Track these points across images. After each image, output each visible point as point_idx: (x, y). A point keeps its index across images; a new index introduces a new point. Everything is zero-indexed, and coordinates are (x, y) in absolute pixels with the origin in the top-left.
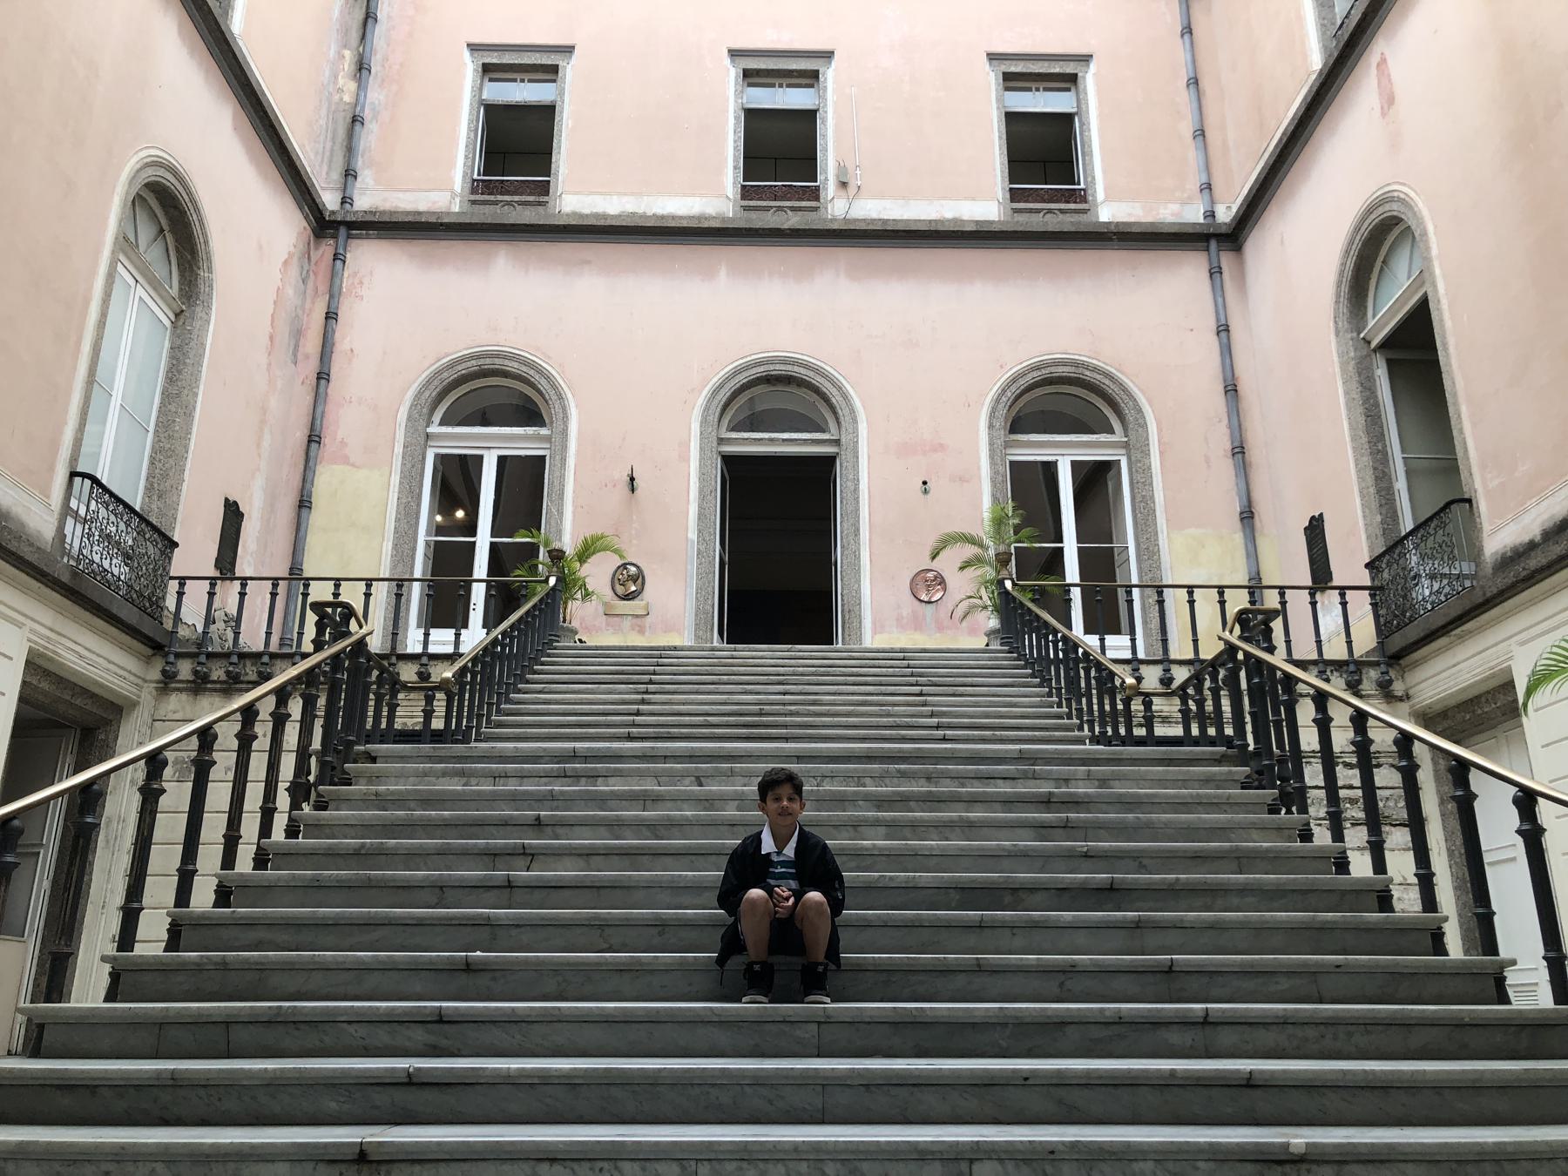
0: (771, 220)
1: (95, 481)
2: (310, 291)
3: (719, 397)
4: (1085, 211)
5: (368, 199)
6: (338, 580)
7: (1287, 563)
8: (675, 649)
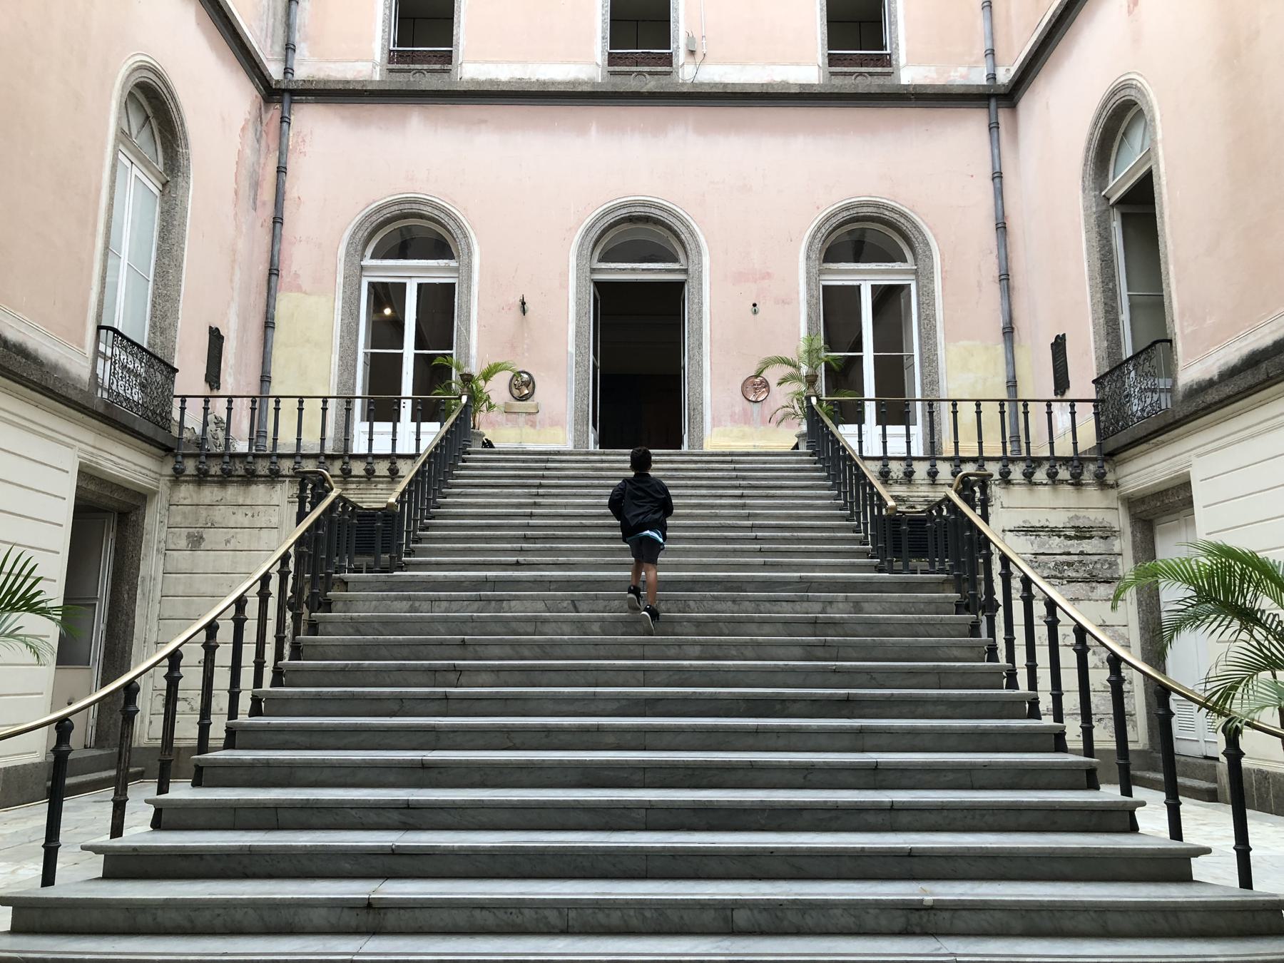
0: (632, 84)
1: (115, 331)
4: (889, 74)
5: (306, 69)
8: (558, 453)
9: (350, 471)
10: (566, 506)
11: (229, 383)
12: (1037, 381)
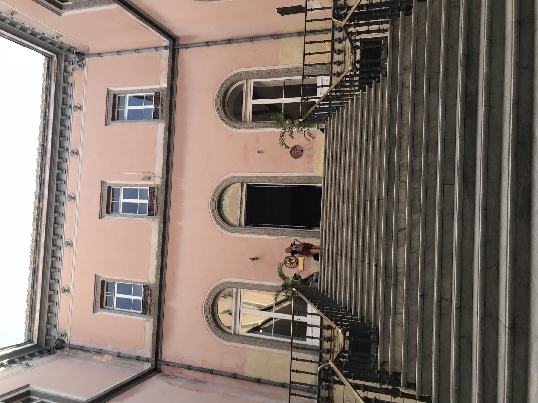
0: (161, 205)
2: (180, 375)
3: (225, 226)
4: (163, 93)
5: (147, 352)
6: (291, 370)
7: (296, 22)
9: (328, 349)
10: (347, 240)
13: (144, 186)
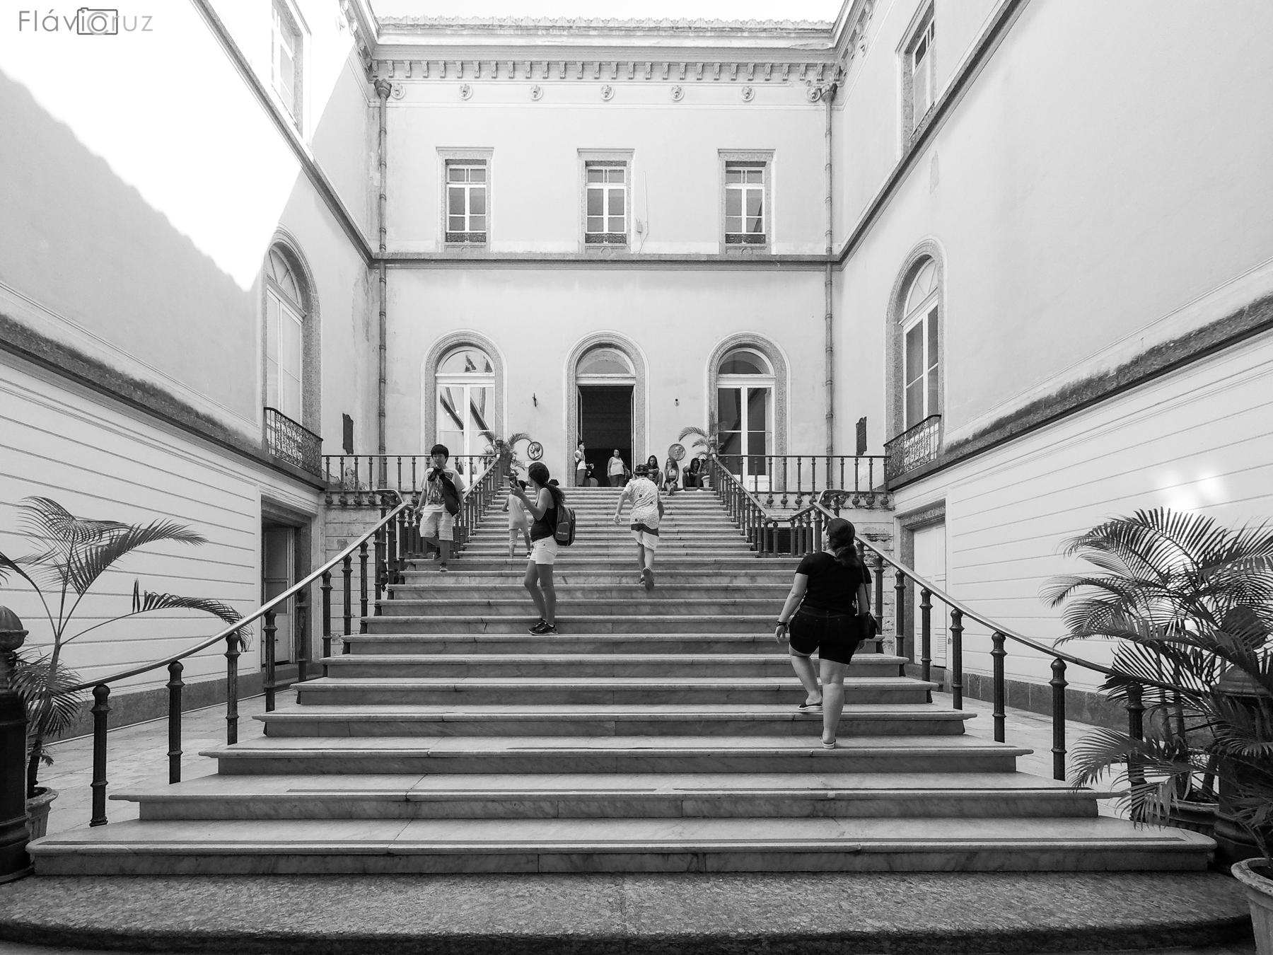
0: (599, 255)
5: (394, 246)
11: (358, 448)
12: (847, 445)
13: (629, 225)
